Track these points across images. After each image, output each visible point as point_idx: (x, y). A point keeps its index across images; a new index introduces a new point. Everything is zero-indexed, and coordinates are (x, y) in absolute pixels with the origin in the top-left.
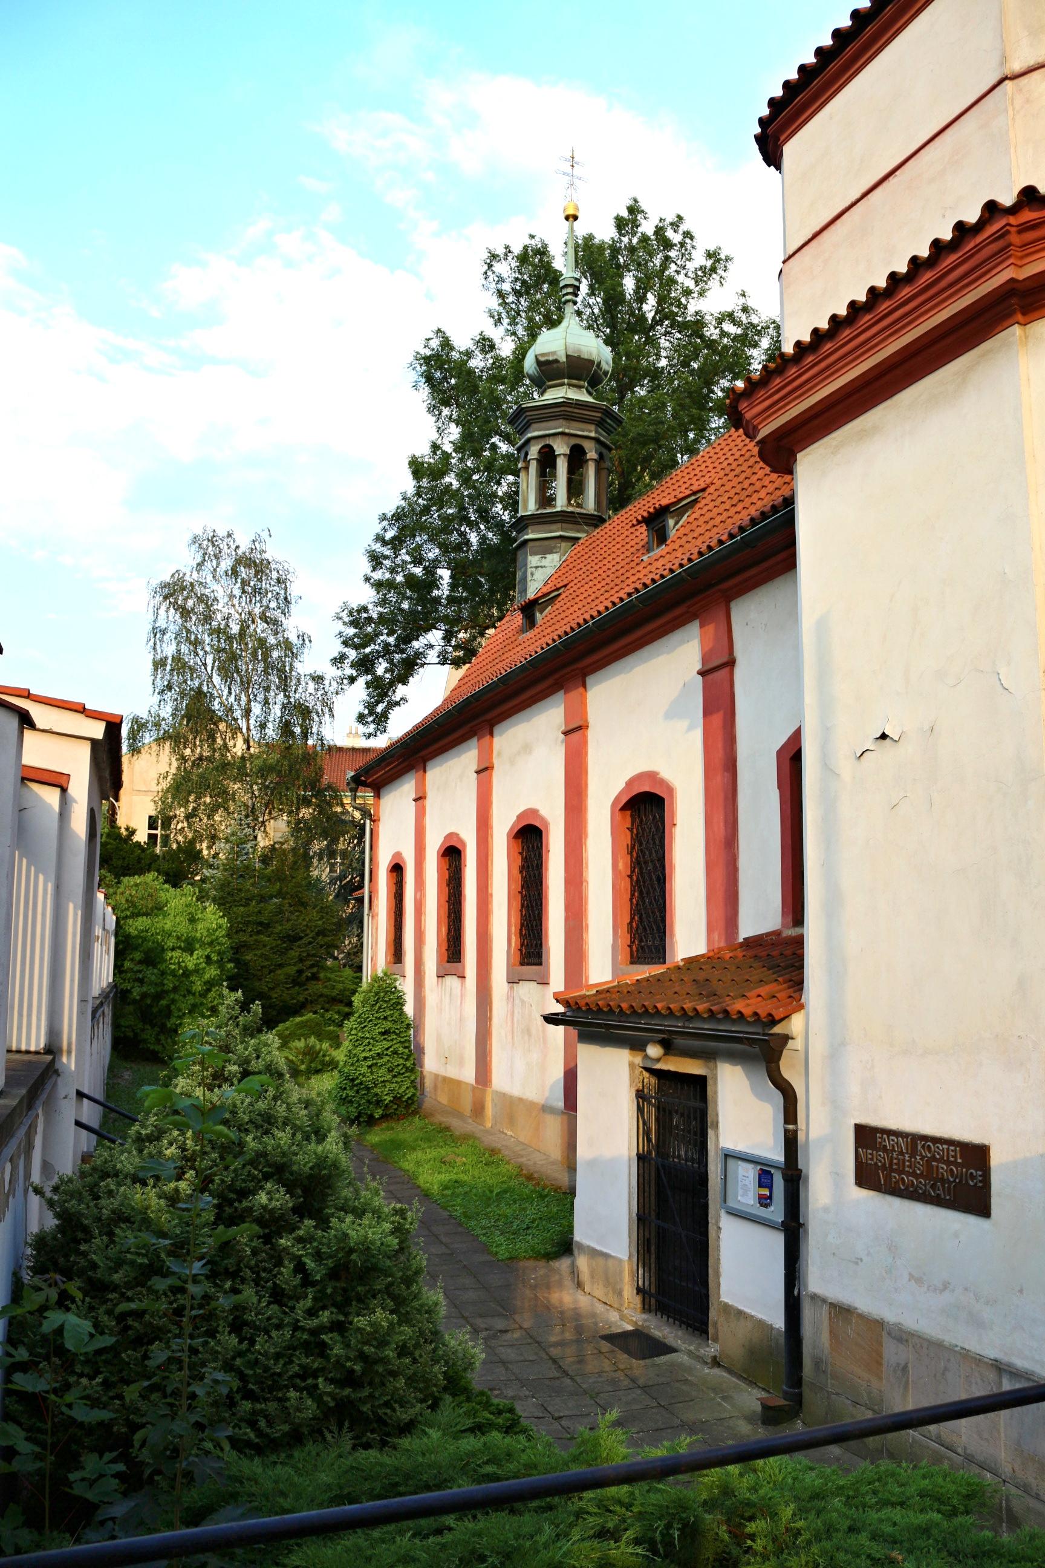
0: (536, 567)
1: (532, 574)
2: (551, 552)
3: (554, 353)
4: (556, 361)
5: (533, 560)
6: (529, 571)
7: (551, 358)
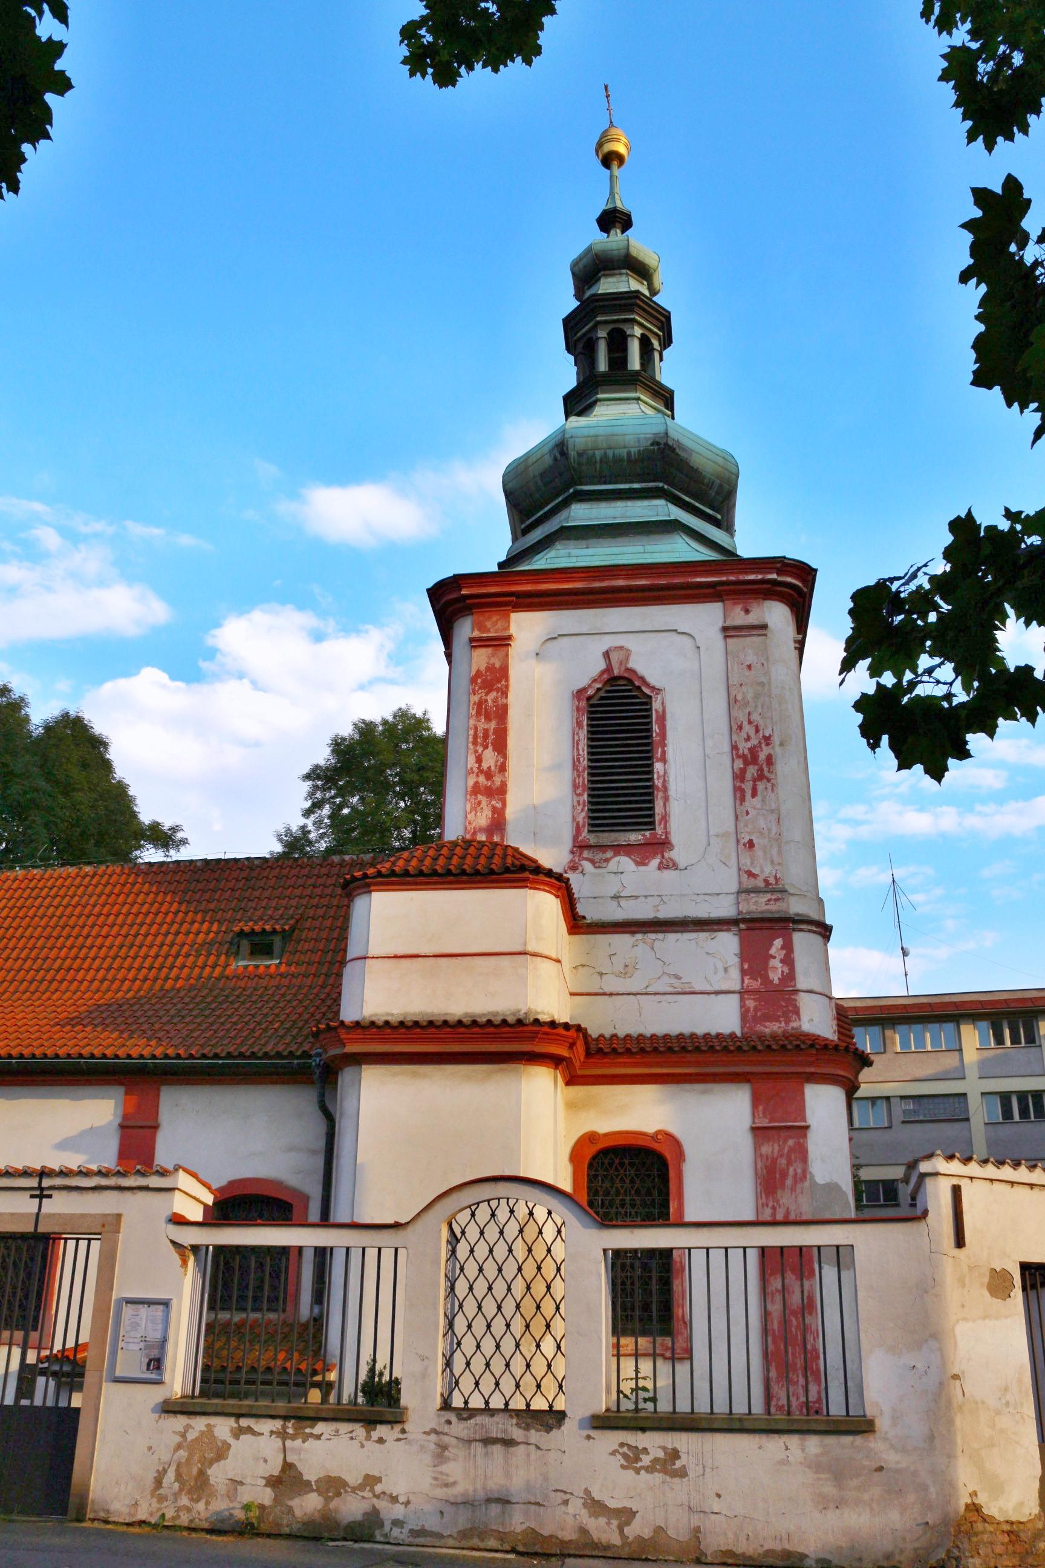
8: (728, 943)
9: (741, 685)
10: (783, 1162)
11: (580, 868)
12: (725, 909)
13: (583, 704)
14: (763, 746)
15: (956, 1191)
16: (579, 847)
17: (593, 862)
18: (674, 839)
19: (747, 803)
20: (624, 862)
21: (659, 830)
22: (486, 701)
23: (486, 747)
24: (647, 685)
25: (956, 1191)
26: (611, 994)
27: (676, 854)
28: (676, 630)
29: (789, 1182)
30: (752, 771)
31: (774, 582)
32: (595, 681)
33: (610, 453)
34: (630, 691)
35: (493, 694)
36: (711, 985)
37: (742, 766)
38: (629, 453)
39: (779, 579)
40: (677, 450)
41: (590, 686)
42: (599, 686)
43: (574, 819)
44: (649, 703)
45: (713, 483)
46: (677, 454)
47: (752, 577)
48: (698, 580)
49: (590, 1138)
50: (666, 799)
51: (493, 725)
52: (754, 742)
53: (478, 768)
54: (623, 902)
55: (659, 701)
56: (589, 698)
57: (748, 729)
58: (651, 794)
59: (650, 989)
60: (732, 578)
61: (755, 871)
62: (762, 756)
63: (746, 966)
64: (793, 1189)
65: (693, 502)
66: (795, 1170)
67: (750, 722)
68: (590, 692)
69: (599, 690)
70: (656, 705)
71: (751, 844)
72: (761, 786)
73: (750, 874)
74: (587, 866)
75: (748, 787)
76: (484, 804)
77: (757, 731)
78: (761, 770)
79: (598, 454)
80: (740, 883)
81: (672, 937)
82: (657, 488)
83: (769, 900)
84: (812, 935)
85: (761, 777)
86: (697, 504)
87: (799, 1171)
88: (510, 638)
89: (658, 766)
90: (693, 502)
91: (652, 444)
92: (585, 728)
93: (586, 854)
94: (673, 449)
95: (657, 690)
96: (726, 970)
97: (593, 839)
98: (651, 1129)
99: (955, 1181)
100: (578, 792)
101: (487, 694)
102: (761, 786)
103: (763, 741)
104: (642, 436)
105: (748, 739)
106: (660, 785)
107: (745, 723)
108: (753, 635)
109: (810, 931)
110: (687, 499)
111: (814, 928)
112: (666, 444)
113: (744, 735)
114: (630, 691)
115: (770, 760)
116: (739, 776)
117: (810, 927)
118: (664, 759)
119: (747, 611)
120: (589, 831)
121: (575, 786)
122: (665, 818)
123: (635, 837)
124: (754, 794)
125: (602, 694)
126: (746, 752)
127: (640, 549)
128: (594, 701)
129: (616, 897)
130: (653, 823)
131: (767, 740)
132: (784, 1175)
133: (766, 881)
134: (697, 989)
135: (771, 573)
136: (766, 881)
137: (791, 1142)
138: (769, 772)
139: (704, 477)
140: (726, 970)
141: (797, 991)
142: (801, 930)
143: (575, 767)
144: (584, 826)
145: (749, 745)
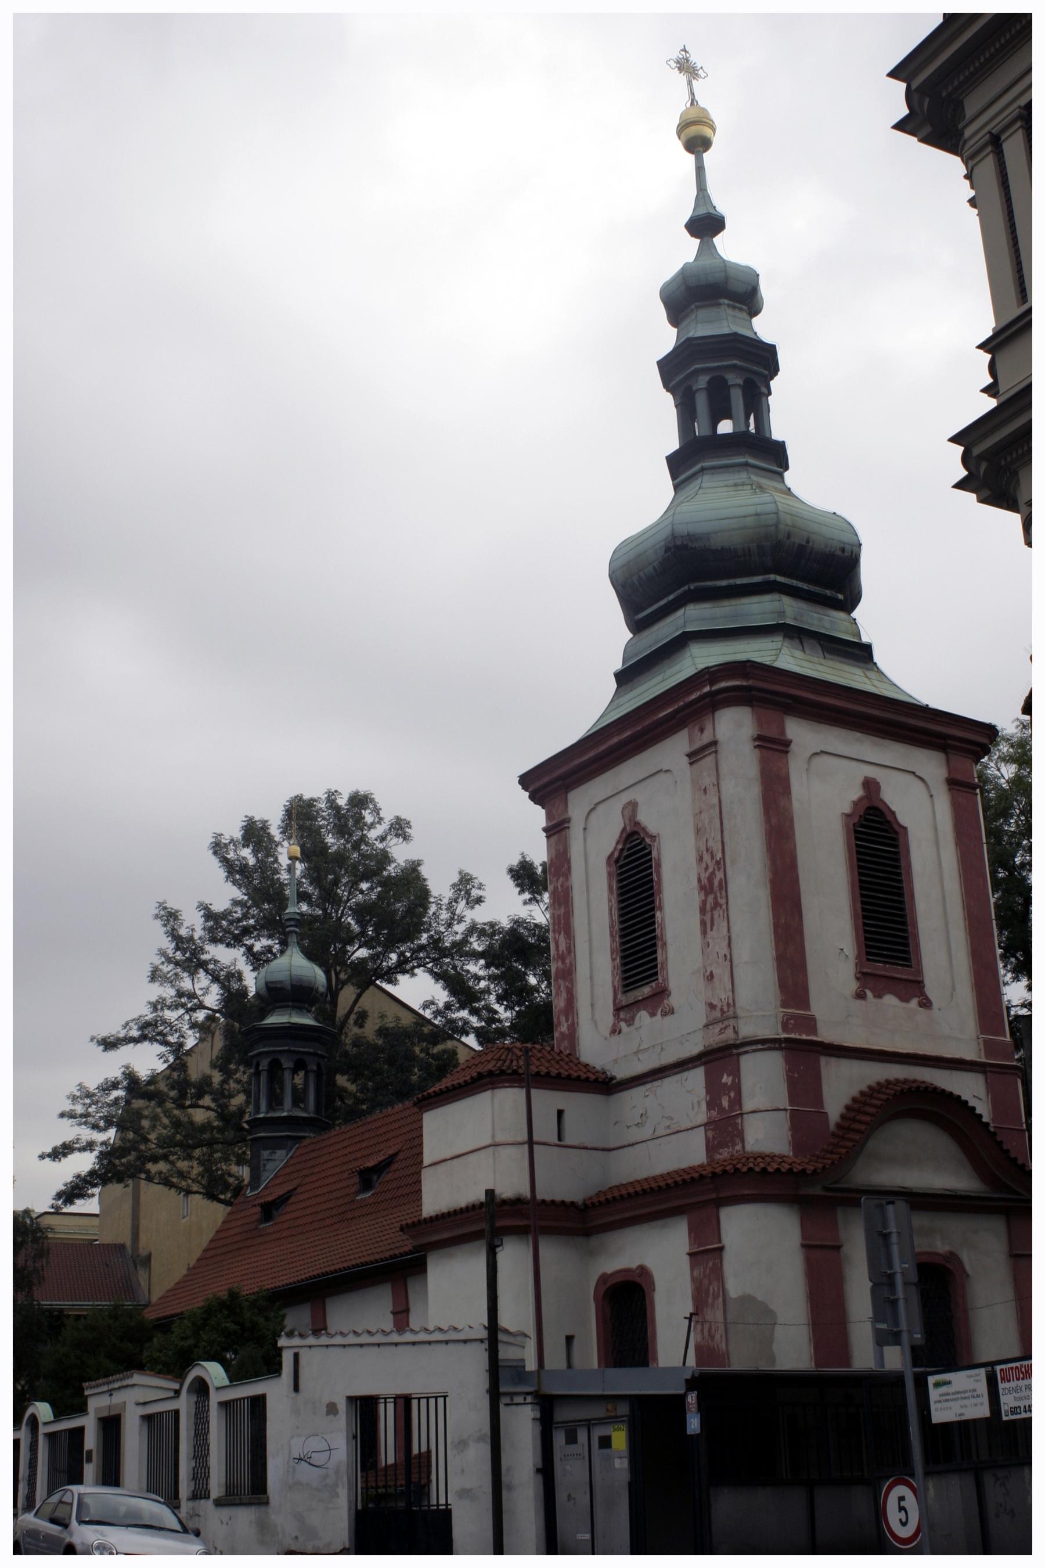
0: (268, 1160)
1: (265, 1165)
2: (280, 1148)
3: (281, 982)
4: (282, 989)
5: (265, 1154)
6: (262, 1163)
7: (278, 986)
8: (697, 1077)
9: (701, 812)
10: (706, 1282)
12: (694, 1048)
13: (614, 868)
14: (716, 871)
15: (296, 1356)
16: (618, 1009)
17: (625, 1020)
18: (673, 985)
19: (708, 936)
20: (643, 1016)
21: (660, 980)
22: (557, 887)
23: (560, 934)
24: (647, 833)
25: (296, 1356)
26: (633, 1144)
27: (675, 1000)
28: (661, 770)
29: (710, 1300)
30: (710, 899)
31: (710, 694)
32: (618, 843)
33: (642, 574)
34: (640, 844)
35: (561, 879)
36: (691, 1121)
37: (704, 898)
38: (654, 568)
39: (714, 688)
40: (690, 544)
41: (615, 849)
42: (620, 847)
43: (613, 982)
44: (650, 853)
45: (749, 549)
46: (692, 548)
47: (694, 696)
48: (661, 715)
49: (604, 1278)
50: (665, 944)
51: (562, 910)
52: (710, 870)
53: (557, 954)
54: (641, 1057)
55: (656, 849)
56: (617, 861)
57: (707, 857)
58: (655, 945)
59: (657, 1134)
60: (681, 703)
61: (715, 1003)
62: (716, 883)
63: (708, 1099)
64: (713, 1306)
65: (732, 582)
66: (713, 1289)
67: (707, 850)
68: (616, 855)
69: (622, 850)
70: (654, 854)
71: (711, 976)
72: (716, 913)
73: (712, 1006)
74: (623, 1024)
75: (708, 918)
76: (562, 986)
77: (712, 858)
78: (716, 898)
79: (635, 579)
80: (707, 1016)
81: (666, 1081)
82: (685, 593)
83: (721, 1030)
84: (759, 1054)
85: (716, 905)
86: (739, 581)
87: (716, 1289)
88: (568, 820)
89: (658, 914)
90: (732, 582)
91: (666, 552)
92: (615, 892)
93: (622, 1015)
94: (684, 547)
95: (653, 838)
96: (699, 1103)
97: (624, 999)
98: (634, 1265)
99: (296, 1350)
100: (614, 957)
101: (557, 880)
105: (707, 868)
107: (705, 852)
108: (706, 756)
109: (755, 1051)
110: (724, 583)
111: (760, 1047)
112: (677, 547)
113: (704, 865)
114: (640, 844)
115: (724, 885)
116: (703, 910)
117: (754, 1047)
118: (660, 908)
119: (702, 730)
121: (612, 953)
122: (665, 963)
123: (646, 991)
125: (625, 853)
126: (706, 881)
127: (659, 678)
128: (621, 863)
129: (636, 1053)
130: (656, 974)
131: (721, 864)
132: (707, 1291)
133: (722, 1010)
134: (683, 1127)
135: (705, 686)
136: (722, 1011)
137: (710, 1264)
138: (721, 898)
140: (699, 1103)
141: (742, 1114)
142: (746, 1052)
143: (612, 935)
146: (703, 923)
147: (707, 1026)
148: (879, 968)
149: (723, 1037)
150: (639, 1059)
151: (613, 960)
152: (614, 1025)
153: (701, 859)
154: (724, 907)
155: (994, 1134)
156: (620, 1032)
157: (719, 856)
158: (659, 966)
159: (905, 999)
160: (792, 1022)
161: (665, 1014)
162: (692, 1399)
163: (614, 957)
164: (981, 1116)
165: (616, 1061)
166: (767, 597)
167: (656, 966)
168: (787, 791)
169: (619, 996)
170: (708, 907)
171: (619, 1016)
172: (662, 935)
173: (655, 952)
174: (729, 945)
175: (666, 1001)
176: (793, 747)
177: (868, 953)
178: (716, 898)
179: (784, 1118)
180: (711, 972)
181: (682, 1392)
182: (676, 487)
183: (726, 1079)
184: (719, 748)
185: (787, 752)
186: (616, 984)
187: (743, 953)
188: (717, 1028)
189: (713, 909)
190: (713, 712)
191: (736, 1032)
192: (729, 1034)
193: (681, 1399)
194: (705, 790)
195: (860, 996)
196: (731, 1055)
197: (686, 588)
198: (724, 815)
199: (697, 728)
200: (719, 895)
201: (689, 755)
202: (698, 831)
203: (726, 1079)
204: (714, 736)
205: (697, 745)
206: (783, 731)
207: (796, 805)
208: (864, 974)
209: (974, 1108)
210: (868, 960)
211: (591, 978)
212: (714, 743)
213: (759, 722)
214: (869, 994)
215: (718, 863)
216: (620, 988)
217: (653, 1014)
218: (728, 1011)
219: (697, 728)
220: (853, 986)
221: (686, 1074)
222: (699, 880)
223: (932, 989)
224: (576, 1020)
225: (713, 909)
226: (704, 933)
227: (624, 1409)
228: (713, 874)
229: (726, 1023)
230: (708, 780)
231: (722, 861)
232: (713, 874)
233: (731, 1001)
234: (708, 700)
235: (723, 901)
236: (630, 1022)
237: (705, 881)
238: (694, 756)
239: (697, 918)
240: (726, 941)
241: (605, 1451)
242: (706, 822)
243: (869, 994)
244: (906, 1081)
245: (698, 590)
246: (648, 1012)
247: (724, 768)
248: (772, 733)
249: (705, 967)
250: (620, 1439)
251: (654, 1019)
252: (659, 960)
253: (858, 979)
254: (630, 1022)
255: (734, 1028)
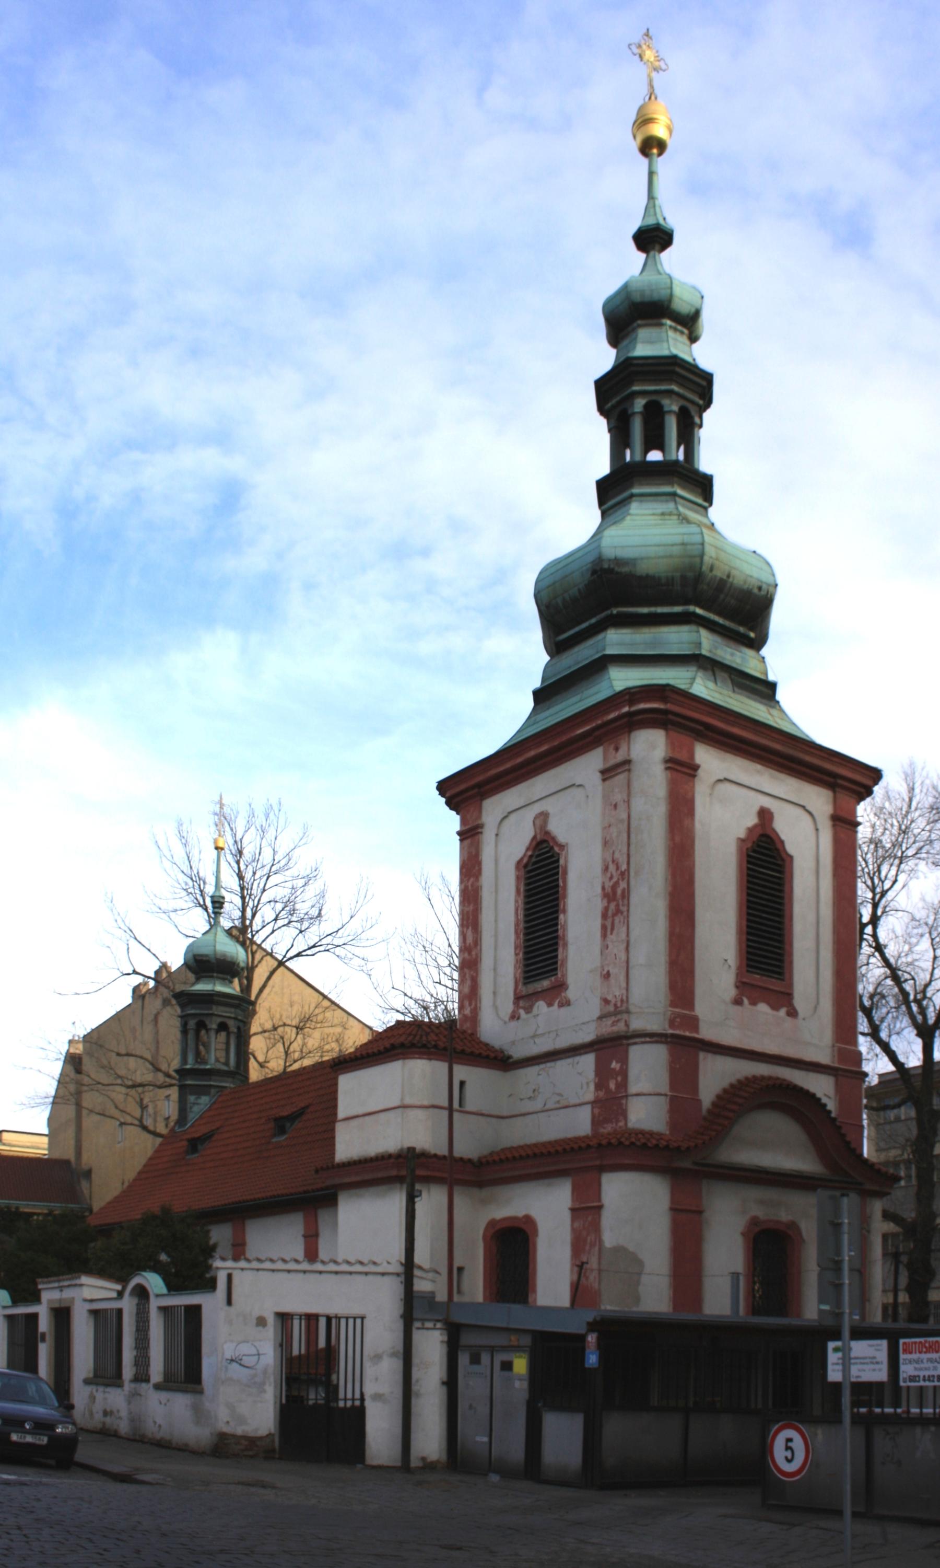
9: (610, 826)
11: (517, 1016)
14: (620, 882)
16: (518, 998)
18: (571, 979)
21: (559, 975)
30: (612, 906)
37: (606, 904)
38: (579, 590)
40: (617, 569)
46: (617, 573)
47: (612, 716)
50: (565, 945)
52: (615, 879)
54: (536, 1040)
57: (612, 868)
60: (599, 722)
62: (619, 892)
65: (652, 609)
67: (613, 861)
73: (606, 1001)
74: (522, 1012)
75: (608, 923)
77: (618, 868)
78: (618, 905)
80: (601, 1010)
85: (618, 911)
89: (561, 917)
90: (652, 609)
93: (521, 1003)
94: (610, 571)
97: (524, 990)
102: (617, 920)
103: (620, 877)
104: (585, 568)
105: (611, 878)
106: (561, 935)
107: (611, 863)
108: (617, 774)
113: (609, 875)
115: (626, 894)
116: (604, 916)
120: (525, 984)
122: (565, 960)
123: (546, 984)
124: (612, 929)
126: (610, 890)
130: (556, 969)
131: (625, 875)
136: (615, 1005)
139: (659, 578)
144: (520, 980)
145: (611, 883)
146: (604, 927)
147: (600, 1018)
148: (756, 979)
149: (615, 1029)
150: (535, 1043)
151: (516, 954)
152: (514, 1012)
153: (606, 869)
154: (625, 913)
155: (840, 1127)
156: (518, 1018)
157: (624, 867)
158: (559, 963)
159: (775, 1007)
160: (678, 1020)
161: (561, 1005)
162: (592, 1338)
163: (517, 952)
164: (830, 1112)
165: (513, 1043)
166: (685, 628)
167: (556, 963)
168: (691, 812)
169: (520, 987)
170: (610, 913)
171: (518, 1005)
172: (564, 935)
173: (556, 950)
174: (627, 949)
175: (563, 994)
176: (700, 772)
177: (748, 966)
178: (618, 905)
179: (662, 1104)
180: (608, 972)
181: (583, 1331)
182: (604, 514)
183: (615, 1065)
184: (633, 767)
185: (694, 776)
186: (518, 976)
187: (639, 956)
188: (609, 1021)
189: (614, 915)
190: (630, 732)
191: (627, 1025)
192: (621, 1027)
193: (582, 1338)
194: (615, 806)
195: (738, 1002)
196: (621, 1045)
197: (608, 612)
198: (632, 830)
199: (612, 746)
200: (621, 903)
201: (603, 772)
202: (606, 843)
203: (615, 1065)
204: (629, 755)
205: (612, 762)
206: (692, 755)
207: (697, 825)
208: (744, 983)
209: (825, 1105)
210: (748, 971)
211: (495, 969)
212: (628, 762)
213: (671, 744)
214: (746, 1001)
215: (622, 874)
216: (522, 980)
217: (550, 1005)
218: (621, 1006)
219: (612, 746)
220: (732, 992)
221: (577, 1059)
222: (603, 888)
223: (800, 1001)
224: (478, 1005)
225: (614, 915)
226: (604, 935)
227: (527, 1340)
228: (617, 883)
229: (619, 1017)
230: (618, 797)
231: (626, 873)
232: (617, 883)
233: (624, 998)
234: (625, 720)
235: (624, 909)
236: (528, 1010)
237: (608, 889)
238: (607, 773)
239: (598, 922)
240: (625, 945)
241: (506, 1373)
242: (615, 835)
243: (746, 1001)
244: (770, 1078)
245: (620, 615)
246: (546, 1003)
247: (636, 786)
248: (682, 756)
249: (602, 967)
250: (521, 1365)
251: (551, 1009)
252: (560, 957)
253: (737, 987)
254: (528, 1010)
255: (626, 1021)
